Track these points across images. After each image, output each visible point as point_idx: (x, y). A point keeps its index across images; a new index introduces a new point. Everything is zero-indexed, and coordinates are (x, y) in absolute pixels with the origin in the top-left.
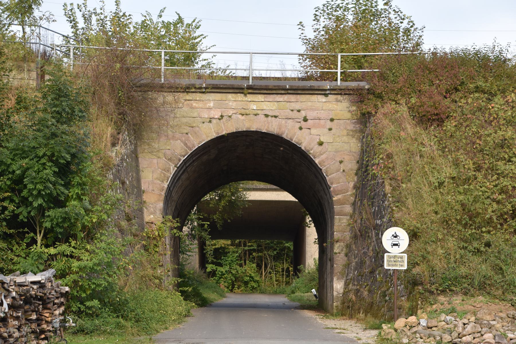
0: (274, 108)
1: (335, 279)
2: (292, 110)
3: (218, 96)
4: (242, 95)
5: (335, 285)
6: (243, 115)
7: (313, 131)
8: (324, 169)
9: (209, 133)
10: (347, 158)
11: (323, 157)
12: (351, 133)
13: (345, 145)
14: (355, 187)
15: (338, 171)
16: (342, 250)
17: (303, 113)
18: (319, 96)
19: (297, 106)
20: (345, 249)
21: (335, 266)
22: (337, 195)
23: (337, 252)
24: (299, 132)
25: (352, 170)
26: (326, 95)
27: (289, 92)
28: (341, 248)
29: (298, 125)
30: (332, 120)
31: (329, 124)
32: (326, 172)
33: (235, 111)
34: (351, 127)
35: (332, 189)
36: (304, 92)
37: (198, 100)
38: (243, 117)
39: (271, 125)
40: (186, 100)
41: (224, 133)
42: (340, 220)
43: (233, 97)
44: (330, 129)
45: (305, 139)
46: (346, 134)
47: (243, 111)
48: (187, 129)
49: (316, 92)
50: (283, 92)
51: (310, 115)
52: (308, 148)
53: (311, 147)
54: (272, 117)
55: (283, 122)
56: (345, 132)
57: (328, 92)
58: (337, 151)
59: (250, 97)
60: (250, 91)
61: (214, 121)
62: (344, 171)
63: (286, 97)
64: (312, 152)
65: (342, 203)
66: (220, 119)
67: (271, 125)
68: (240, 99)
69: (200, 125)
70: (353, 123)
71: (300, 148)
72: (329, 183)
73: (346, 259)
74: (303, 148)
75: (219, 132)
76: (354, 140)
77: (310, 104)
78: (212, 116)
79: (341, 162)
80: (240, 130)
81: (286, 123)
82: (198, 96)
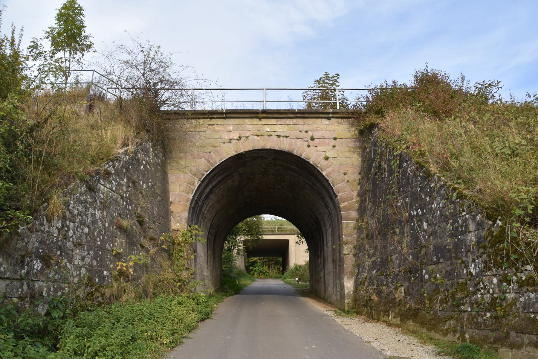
0: (285, 130)
1: (345, 278)
2: (301, 131)
3: (237, 121)
4: (258, 120)
5: (345, 284)
6: (258, 136)
7: (320, 148)
8: (330, 180)
9: (229, 151)
10: (350, 170)
11: (329, 169)
12: (352, 149)
13: (348, 159)
14: (358, 195)
15: (343, 181)
16: (351, 252)
17: (310, 134)
18: (323, 120)
19: (305, 128)
20: (353, 251)
21: (345, 266)
22: (344, 202)
23: (346, 253)
24: (307, 149)
25: (355, 180)
26: (329, 118)
27: (298, 115)
28: (349, 249)
29: (307, 143)
30: (335, 139)
31: (333, 142)
32: (333, 182)
33: (251, 133)
34: (352, 144)
35: (338, 197)
36: (310, 116)
37: (220, 125)
38: (259, 138)
39: (282, 143)
40: (209, 125)
41: (242, 151)
42: (347, 224)
43: (249, 122)
44: (334, 147)
45: (313, 155)
46: (348, 150)
47: (258, 133)
48: (210, 149)
49: (321, 116)
50: (292, 116)
51: (316, 135)
52: (316, 163)
53: (318, 161)
54: (283, 137)
55: (294, 141)
56: (347, 149)
57: (331, 115)
58: (341, 165)
59: (264, 121)
60: (264, 115)
61: (233, 141)
62: (348, 181)
63: (295, 121)
64: (319, 165)
65: (348, 209)
66: (238, 140)
67: (282, 143)
68: (255, 123)
69: (221, 145)
70: (354, 141)
71: (309, 162)
72: (335, 192)
73: (354, 259)
74: (311, 163)
75: (238, 150)
76: (355, 155)
77: (315, 126)
78: (231, 137)
79: (345, 174)
80: (256, 148)
81: (296, 142)
82: (220, 121)
